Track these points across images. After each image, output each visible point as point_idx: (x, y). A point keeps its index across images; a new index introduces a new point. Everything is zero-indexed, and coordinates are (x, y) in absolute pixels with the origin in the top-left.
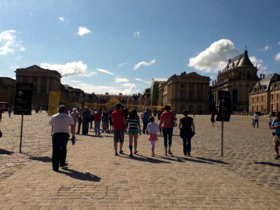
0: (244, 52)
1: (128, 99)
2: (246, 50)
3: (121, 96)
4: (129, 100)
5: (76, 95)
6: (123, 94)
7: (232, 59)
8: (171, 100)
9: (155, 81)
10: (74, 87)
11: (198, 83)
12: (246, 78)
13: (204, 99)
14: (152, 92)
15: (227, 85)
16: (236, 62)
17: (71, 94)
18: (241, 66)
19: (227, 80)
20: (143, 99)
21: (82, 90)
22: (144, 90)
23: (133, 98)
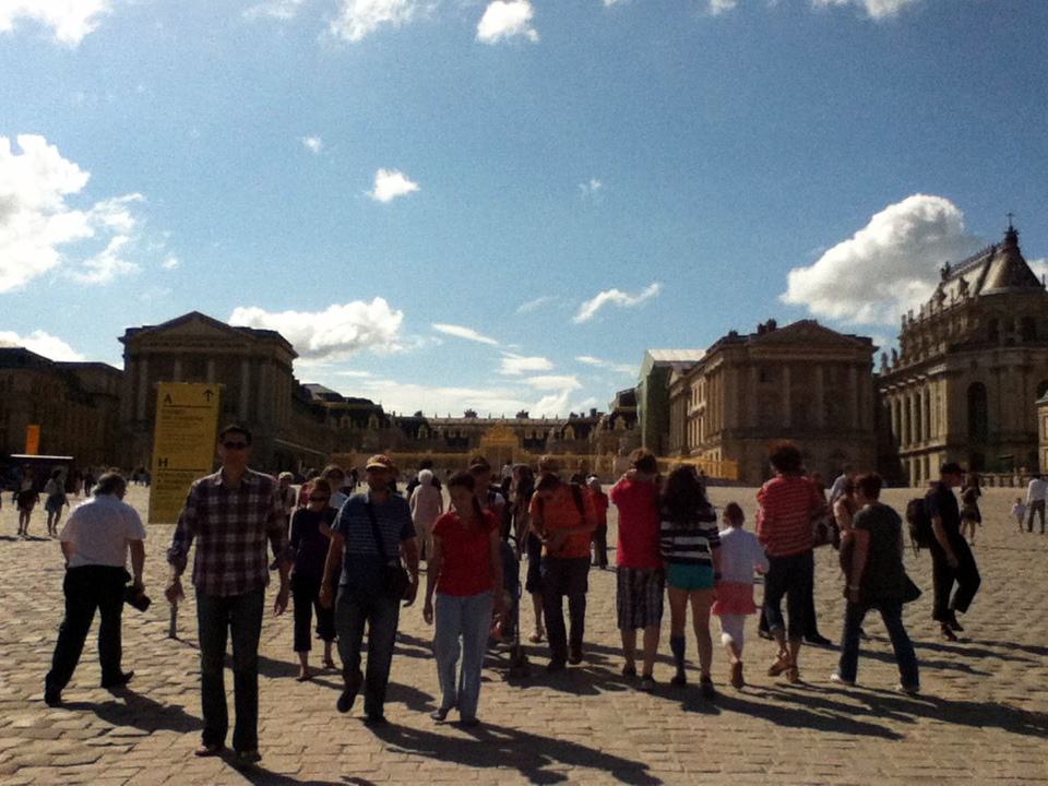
0: (1005, 236)
1: (552, 432)
2: (1011, 228)
3: (525, 421)
4: (556, 435)
5: (355, 423)
6: (530, 416)
7: (958, 266)
8: (724, 432)
9: (655, 362)
10: (345, 394)
11: (826, 365)
12: (1018, 339)
13: (855, 424)
14: (642, 406)
15: (941, 368)
16: (972, 278)
17: (333, 421)
18: (1000, 290)
19: (943, 348)
20: (609, 431)
21: (376, 403)
22: (613, 398)
23: (570, 430)
